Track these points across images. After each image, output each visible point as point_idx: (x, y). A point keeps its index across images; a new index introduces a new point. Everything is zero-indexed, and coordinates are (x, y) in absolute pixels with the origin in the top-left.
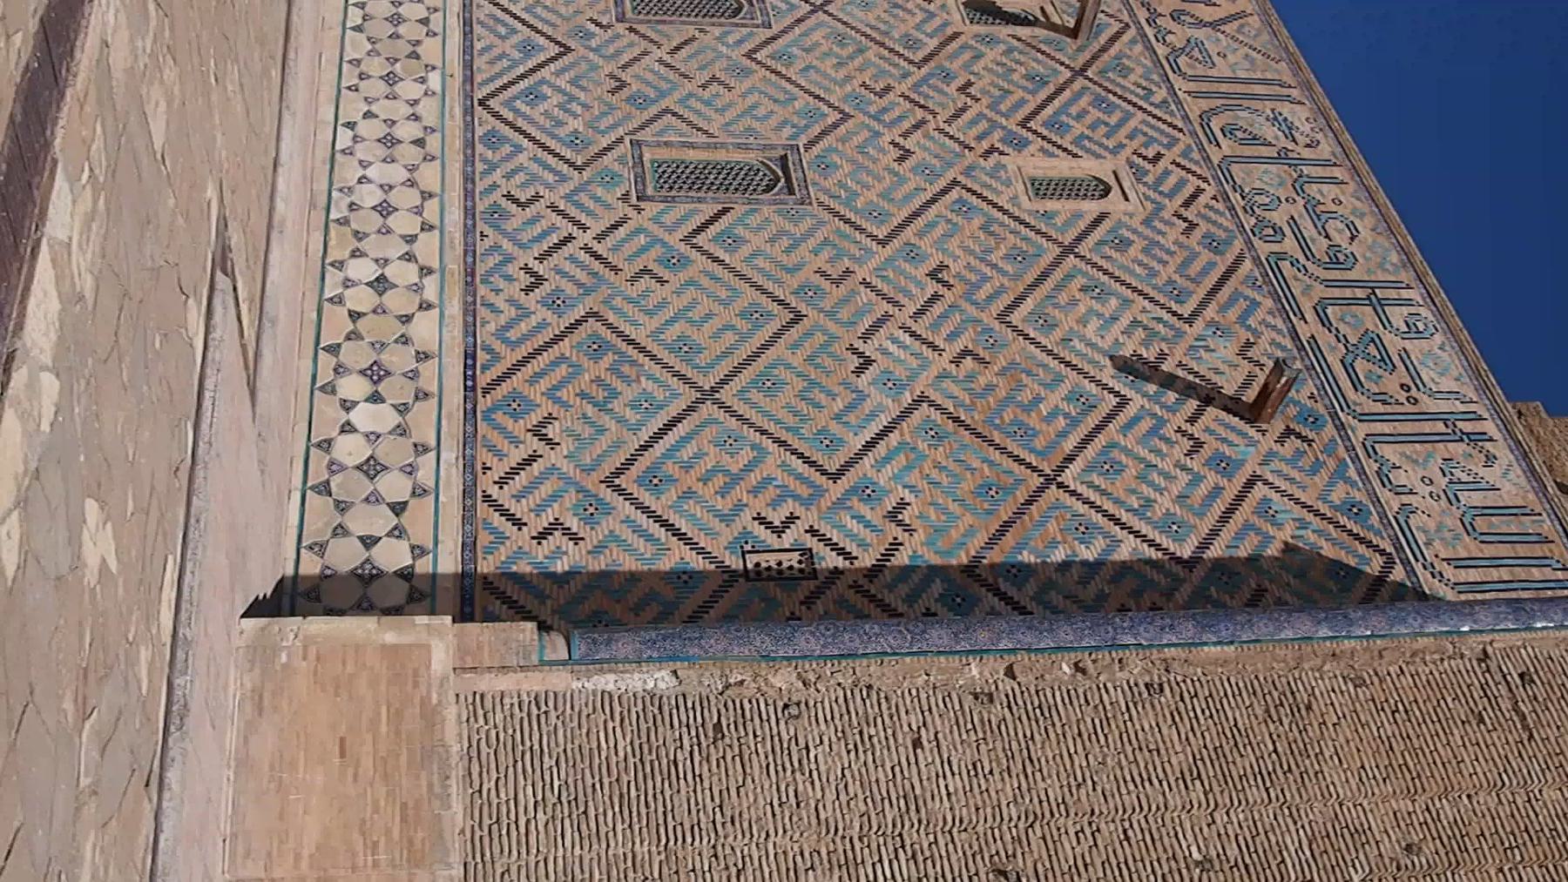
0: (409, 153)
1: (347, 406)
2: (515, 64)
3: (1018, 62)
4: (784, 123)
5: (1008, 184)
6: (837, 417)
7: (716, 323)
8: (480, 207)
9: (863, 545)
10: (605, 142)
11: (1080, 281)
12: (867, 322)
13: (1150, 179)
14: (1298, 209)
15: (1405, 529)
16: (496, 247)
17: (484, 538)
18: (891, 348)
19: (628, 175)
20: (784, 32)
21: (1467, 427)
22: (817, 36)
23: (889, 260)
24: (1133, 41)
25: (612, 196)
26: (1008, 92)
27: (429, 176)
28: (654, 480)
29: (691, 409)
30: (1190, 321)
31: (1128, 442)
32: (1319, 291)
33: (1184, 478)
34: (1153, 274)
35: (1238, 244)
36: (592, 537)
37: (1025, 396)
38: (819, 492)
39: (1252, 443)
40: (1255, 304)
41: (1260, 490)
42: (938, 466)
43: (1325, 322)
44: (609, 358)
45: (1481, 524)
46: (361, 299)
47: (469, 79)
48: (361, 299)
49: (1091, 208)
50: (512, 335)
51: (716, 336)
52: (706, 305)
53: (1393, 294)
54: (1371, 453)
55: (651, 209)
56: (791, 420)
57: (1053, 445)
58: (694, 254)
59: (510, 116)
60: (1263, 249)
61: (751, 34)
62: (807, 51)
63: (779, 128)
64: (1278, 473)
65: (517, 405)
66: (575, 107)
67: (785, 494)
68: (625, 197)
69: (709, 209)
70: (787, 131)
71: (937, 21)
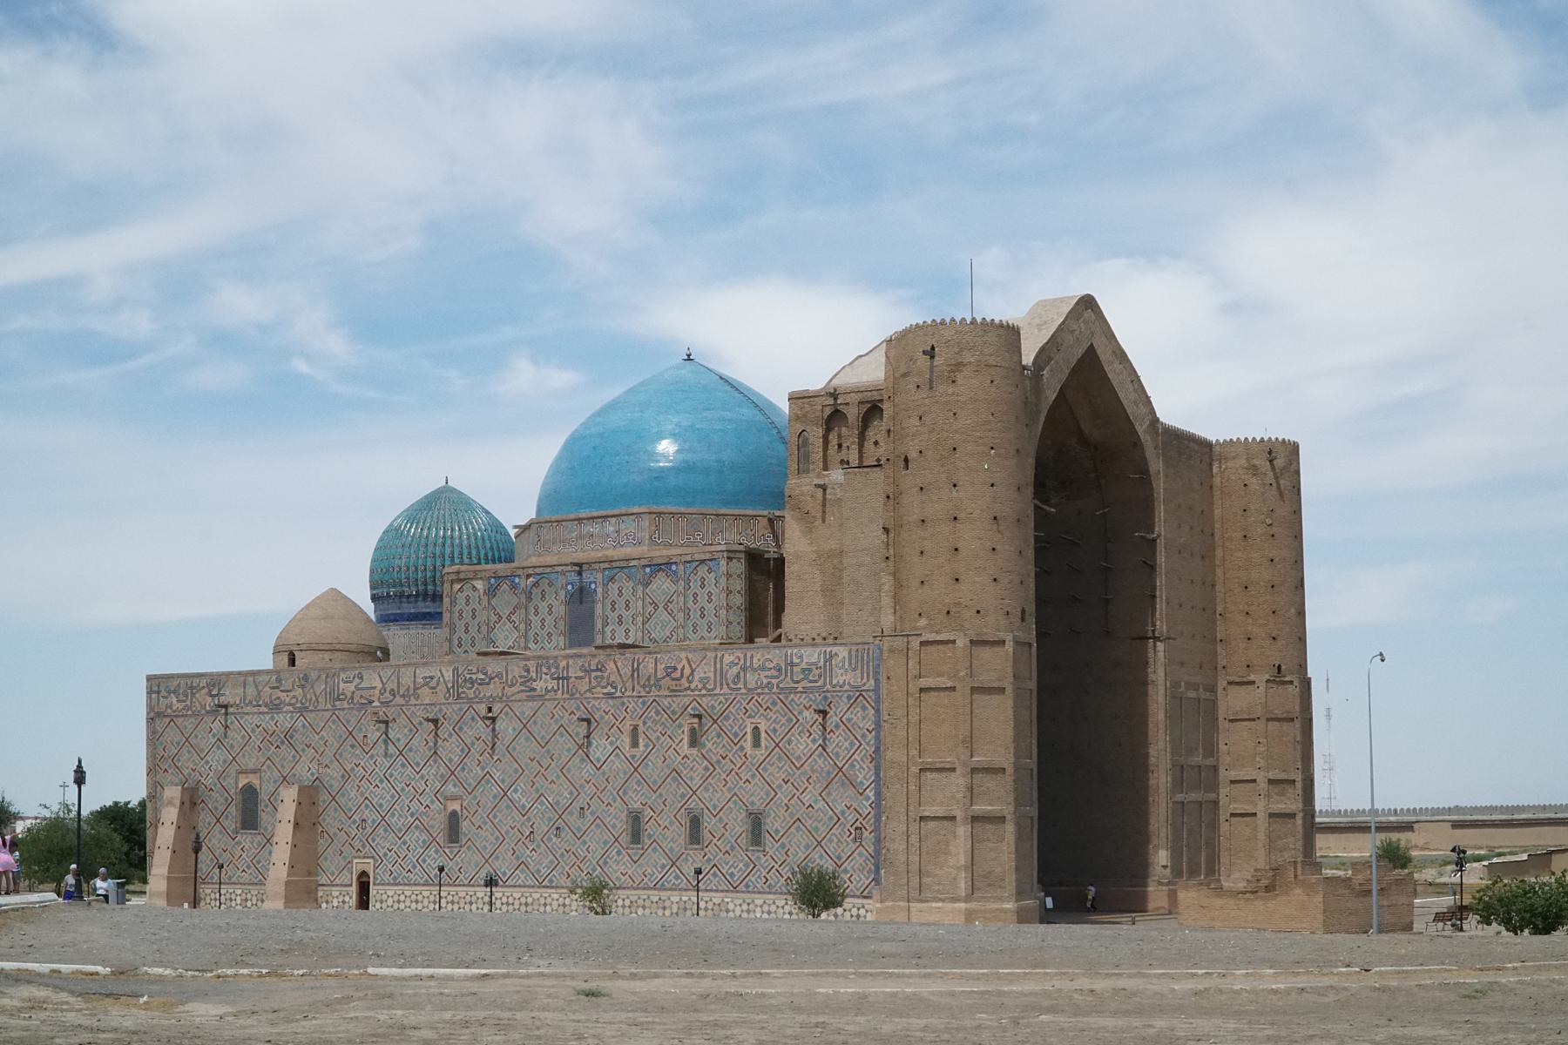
0: (752, 907)
3: (712, 739)
4: (738, 811)
5: (756, 755)
6: (825, 815)
8: (768, 890)
9: (855, 816)
10: (747, 859)
12: (799, 802)
13: (753, 714)
14: (763, 674)
15: (853, 687)
16: (780, 888)
18: (806, 798)
19: (757, 854)
20: (704, 804)
21: (828, 657)
22: (706, 796)
23: (782, 793)
24: (701, 699)
26: (724, 746)
27: (759, 902)
28: (839, 858)
29: (822, 847)
30: (798, 720)
31: (831, 748)
32: (788, 679)
33: (840, 738)
34: (783, 724)
36: (852, 872)
37: (819, 769)
38: (842, 823)
39: (831, 717)
40: (793, 700)
41: (844, 719)
42: (837, 795)
43: (798, 682)
47: (727, 891)
49: (763, 735)
51: (804, 839)
52: (795, 840)
53: (789, 658)
54: (834, 686)
55: (767, 849)
57: (832, 766)
59: (739, 882)
60: (775, 690)
61: (707, 814)
62: (711, 800)
63: (740, 813)
64: (840, 713)
66: (736, 864)
67: (843, 830)
68: (765, 856)
69: (767, 835)
70: (741, 811)
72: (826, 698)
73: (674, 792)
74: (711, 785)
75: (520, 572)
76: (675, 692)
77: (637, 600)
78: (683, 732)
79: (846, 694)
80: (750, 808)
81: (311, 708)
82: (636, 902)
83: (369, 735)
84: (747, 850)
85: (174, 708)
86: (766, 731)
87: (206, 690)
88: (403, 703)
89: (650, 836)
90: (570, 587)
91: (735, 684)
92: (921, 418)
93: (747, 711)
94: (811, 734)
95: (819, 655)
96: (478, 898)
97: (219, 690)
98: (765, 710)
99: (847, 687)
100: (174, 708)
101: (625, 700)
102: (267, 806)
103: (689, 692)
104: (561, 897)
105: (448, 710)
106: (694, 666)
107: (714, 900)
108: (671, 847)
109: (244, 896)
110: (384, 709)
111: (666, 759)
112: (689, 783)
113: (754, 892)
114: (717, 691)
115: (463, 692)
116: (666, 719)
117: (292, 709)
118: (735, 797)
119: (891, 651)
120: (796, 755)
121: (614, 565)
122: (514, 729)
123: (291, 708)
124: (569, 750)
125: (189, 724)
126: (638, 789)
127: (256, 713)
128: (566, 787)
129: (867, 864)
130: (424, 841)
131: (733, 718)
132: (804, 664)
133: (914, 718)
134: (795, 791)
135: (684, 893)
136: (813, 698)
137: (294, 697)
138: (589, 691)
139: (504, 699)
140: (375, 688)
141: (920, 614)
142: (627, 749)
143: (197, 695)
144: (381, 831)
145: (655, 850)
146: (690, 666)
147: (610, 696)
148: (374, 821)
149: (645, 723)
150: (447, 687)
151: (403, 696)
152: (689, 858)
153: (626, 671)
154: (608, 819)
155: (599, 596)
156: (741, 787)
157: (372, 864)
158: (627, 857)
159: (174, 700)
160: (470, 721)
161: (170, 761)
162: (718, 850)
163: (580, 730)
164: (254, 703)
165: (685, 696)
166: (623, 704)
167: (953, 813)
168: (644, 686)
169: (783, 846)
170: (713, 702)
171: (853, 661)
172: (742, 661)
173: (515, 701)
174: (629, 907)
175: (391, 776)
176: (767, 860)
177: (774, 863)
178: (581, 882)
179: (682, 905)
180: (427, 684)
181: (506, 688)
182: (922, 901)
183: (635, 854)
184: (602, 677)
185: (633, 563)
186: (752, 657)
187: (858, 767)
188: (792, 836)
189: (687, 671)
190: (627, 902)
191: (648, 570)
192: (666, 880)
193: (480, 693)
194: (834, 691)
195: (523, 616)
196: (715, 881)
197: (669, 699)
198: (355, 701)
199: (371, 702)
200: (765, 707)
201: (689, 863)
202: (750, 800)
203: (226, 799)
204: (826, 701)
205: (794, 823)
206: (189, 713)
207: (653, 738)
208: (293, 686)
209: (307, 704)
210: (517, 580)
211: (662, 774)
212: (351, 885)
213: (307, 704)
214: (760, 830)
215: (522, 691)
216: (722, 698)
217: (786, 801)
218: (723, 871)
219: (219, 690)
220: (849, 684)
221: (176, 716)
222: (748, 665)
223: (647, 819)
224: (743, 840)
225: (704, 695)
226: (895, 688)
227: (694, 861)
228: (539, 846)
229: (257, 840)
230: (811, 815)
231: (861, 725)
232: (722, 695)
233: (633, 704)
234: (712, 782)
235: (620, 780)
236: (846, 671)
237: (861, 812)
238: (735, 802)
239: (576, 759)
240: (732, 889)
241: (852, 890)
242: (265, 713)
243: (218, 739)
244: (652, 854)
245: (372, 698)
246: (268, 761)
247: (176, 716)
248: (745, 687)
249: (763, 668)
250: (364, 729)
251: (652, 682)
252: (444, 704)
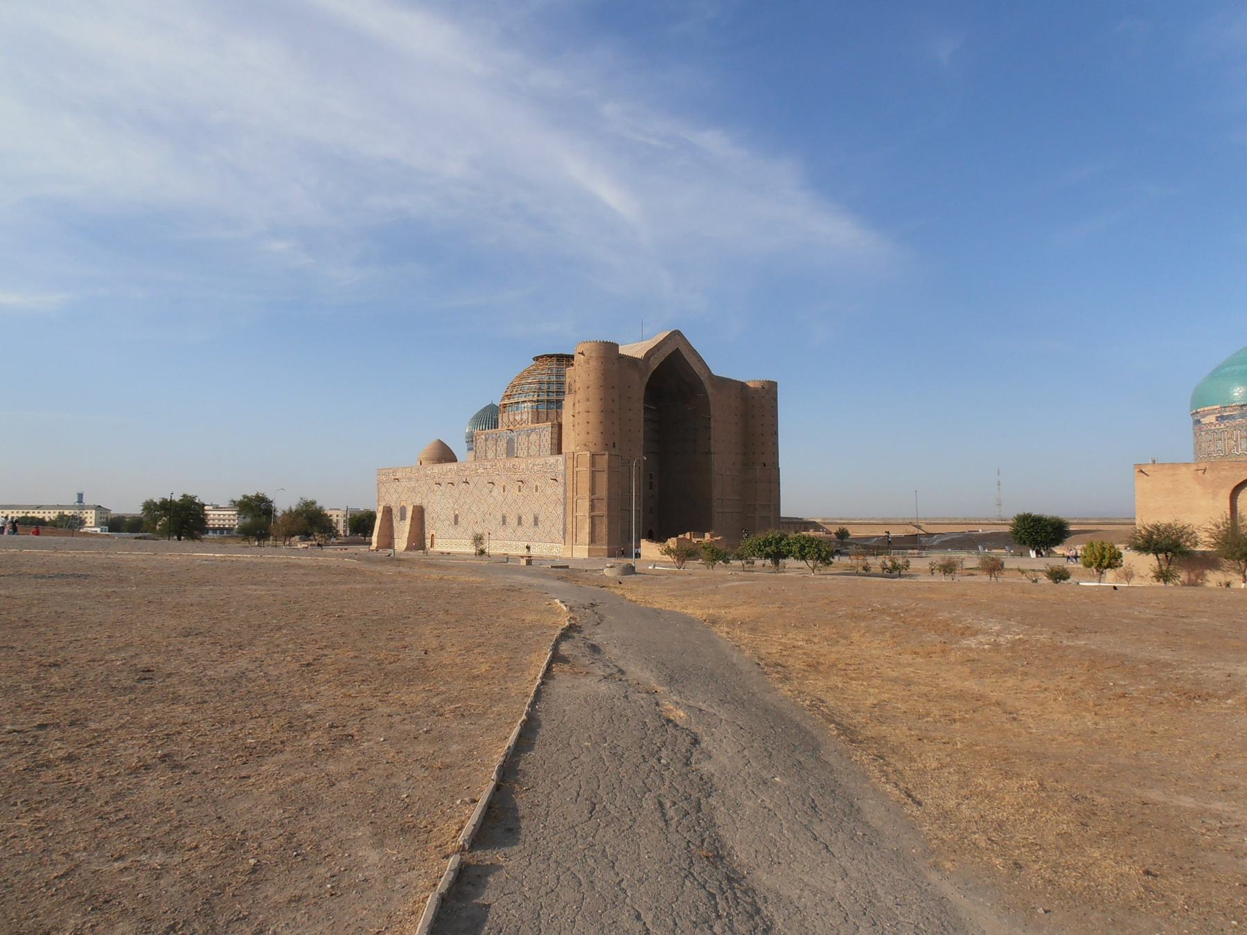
125: (387, 485)
133: (575, 482)
153: (502, 466)
155: (516, 440)
249: (538, 464)
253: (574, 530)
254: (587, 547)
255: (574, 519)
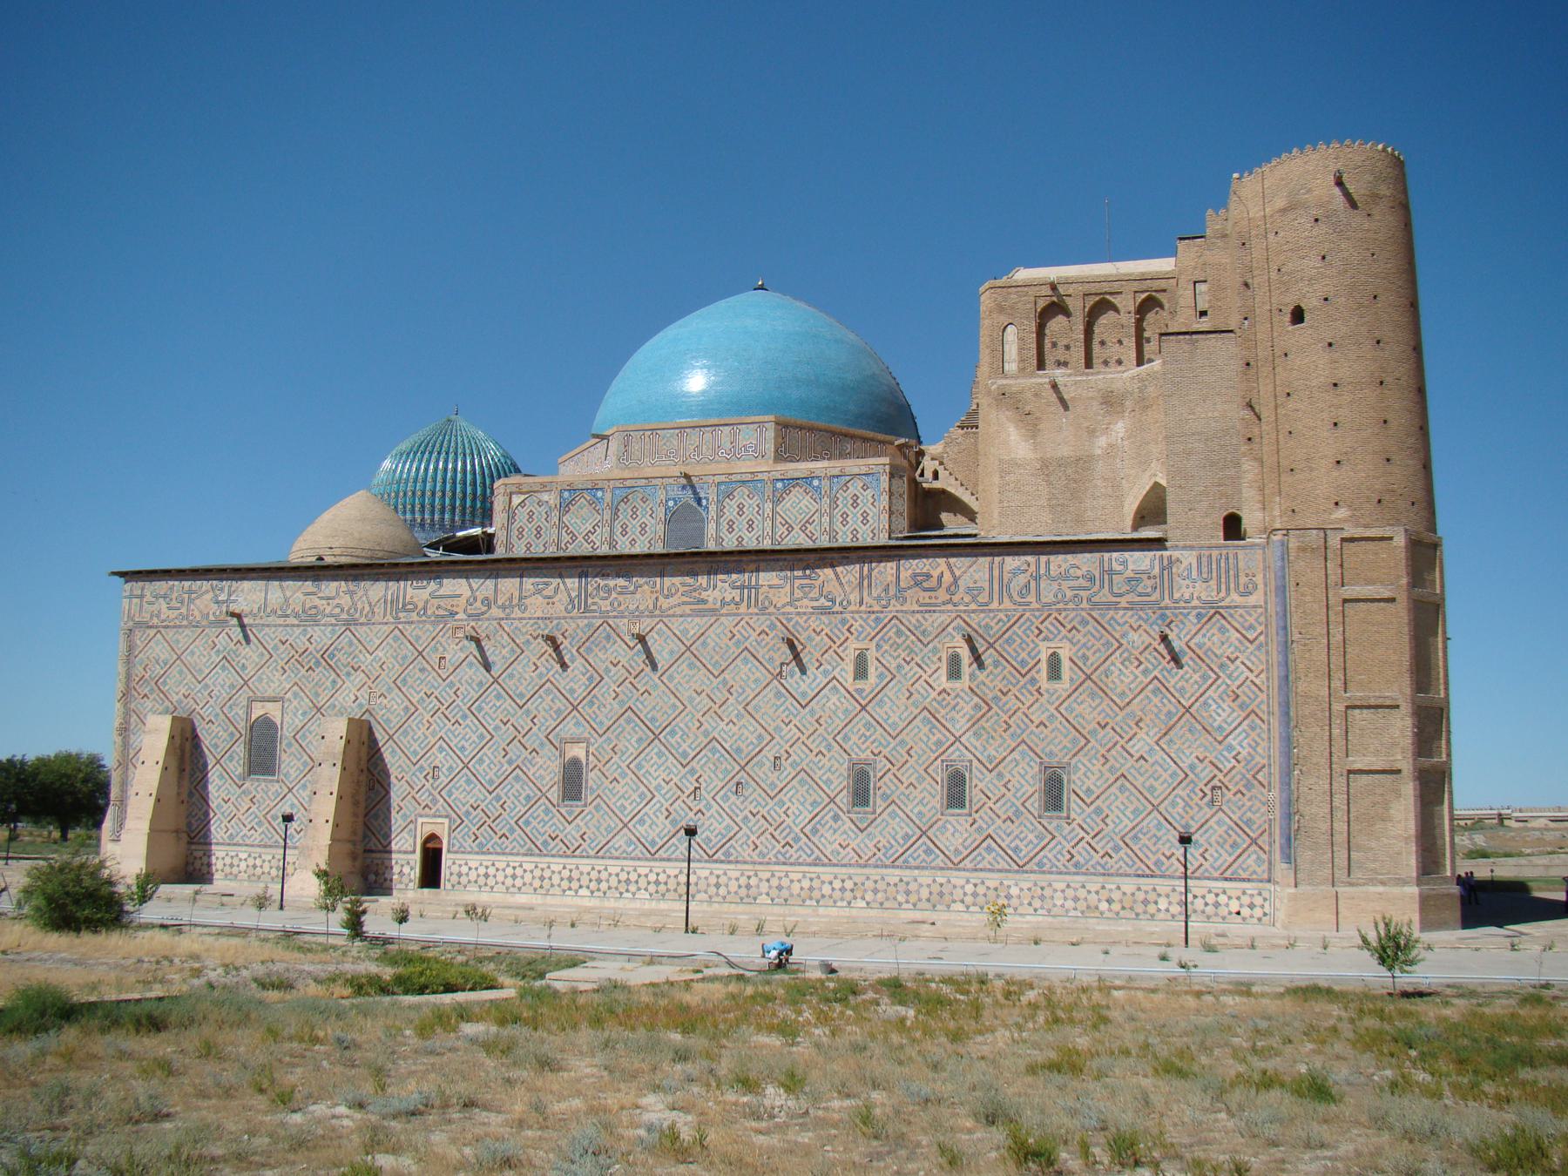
0: (1047, 892)
1: (1159, 910)
2: (998, 855)
5: (1056, 691)
7: (1126, 801)
11: (1103, 677)
12: (1125, 754)
13: (1051, 636)
14: (1066, 584)
17: (1207, 874)
18: (1137, 747)
19: (1055, 823)
21: (1166, 562)
22: (978, 744)
25: (1069, 828)
27: (1062, 886)
30: (1121, 645)
31: (1173, 682)
34: (1099, 650)
35: (1084, 614)
38: (1192, 781)
40: (1112, 618)
41: (1192, 644)
43: (1121, 595)
44: (1140, 835)
45: (1205, 576)
46: (1116, 907)
48: (1116, 907)
49: (1066, 665)
50: (1130, 863)
52: (1118, 803)
55: (1073, 815)
56: (1166, 785)
58: (1095, 805)
60: (1085, 605)
62: (985, 749)
65: (1158, 863)
69: (1073, 797)
71: (962, 694)
72: (1163, 617)
73: (925, 739)
74: (984, 728)
75: (605, 485)
76: (929, 609)
77: (764, 520)
78: (940, 659)
79: (1194, 612)
80: (1046, 759)
81: (363, 620)
82: (863, 884)
83: (448, 657)
84: (1040, 817)
85: (163, 617)
86: (1071, 659)
87: (211, 595)
88: (502, 615)
89: (885, 797)
90: (671, 503)
91: (1020, 594)
92: (1324, 258)
93: (1041, 632)
94: (1141, 663)
95: (1152, 561)
96: (610, 875)
97: (230, 595)
98: (1070, 631)
99: (1195, 602)
100: (163, 617)
101: (848, 616)
102: (289, 745)
103: (950, 607)
104: (742, 875)
105: (570, 626)
106: (958, 573)
107: (988, 883)
108: (920, 813)
109: (251, 862)
110: (473, 624)
111: (911, 694)
112: (949, 725)
113: (1050, 873)
114: (992, 606)
115: (594, 604)
116: (912, 642)
117: (334, 621)
118: (1023, 746)
119: (1302, 549)
120: (1119, 690)
121: (734, 478)
122: (672, 652)
123: (334, 621)
124: (756, 681)
125: (184, 638)
126: (868, 734)
127: (280, 625)
128: (751, 728)
129: (1230, 836)
130: (528, 798)
131: (1019, 641)
132: (1129, 571)
133: (1337, 638)
134: (1118, 738)
135: (939, 873)
136: (1144, 616)
137: (337, 606)
138: (788, 603)
139: (657, 612)
140: (460, 596)
141: (1337, 504)
142: (850, 679)
143: (197, 602)
144: (462, 782)
145: (893, 815)
146: (952, 572)
147: (825, 611)
148: (450, 769)
149: (878, 646)
150: (569, 596)
151: (503, 607)
152: (949, 826)
154: (820, 773)
156: (1032, 732)
157: (446, 825)
158: (849, 824)
159: (164, 606)
160: (604, 642)
161: (153, 684)
162: (994, 816)
163: (776, 656)
164: (279, 612)
165: (940, 611)
166: (844, 621)
167: (1398, 766)
168: (878, 599)
169: (1098, 811)
170: (987, 620)
171: (1205, 570)
172: (1033, 568)
173: (673, 616)
174: (852, 890)
175: (480, 709)
176: (1073, 829)
177: (1082, 834)
178: (775, 856)
179: (935, 888)
180: (539, 592)
181: (661, 598)
182: (1351, 884)
183: (861, 820)
184: (811, 587)
185: (760, 476)
186: (1048, 562)
187: (1214, 706)
188: (1113, 797)
189: (947, 578)
190: (849, 884)
191: (779, 485)
192: (911, 855)
193: (620, 605)
194: (1175, 608)
195: (606, 535)
196: (989, 858)
197: (918, 616)
198: (429, 612)
199: (452, 614)
200: (1069, 627)
201: (948, 834)
202: (1047, 750)
203: (232, 734)
204: (1164, 620)
205: (1117, 779)
206: (185, 623)
207: (892, 667)
208: (338, 594)
209: (357, 615)
210: (599, 494)
211: (906, 714)
212: (414, 852)
213: (357, 615)
214: (1061, 789)
215: (684, 603)
216: (1001, 615)
217: (1103, 751)
218: (1003, 845)
219: (230, 595)
220: (1199, 598)
221: (165, 627)
222: (1042, 571)
223: (880, 774)
224: (1035, 804)
225: (974, 611)
226: (1308, 598)
227: (956, 830)
228: (709, 807)
229: (273, 790)
230: (1142, 770)
231: (1218, 652)
232: (1000, 610)
233: (860, 622)
234: (986, 725)
235: (838, 721)
236: (1194, 581)
237: (1220, 766)
238: (1022, 753)
239: (769, 693)
240: (1016, 867)
241: (1207, 870)
242: (293, 625)
243: (224, 657)
244: (890, 821)
245: (455, 609)
246: (295, 688)
247: (165, 627)
248: (1038, 599)
250: (441, 649)
251: (892, 591)
252: (565, 618)
253: (1340, 826)
254: (1413, 890)
255: (1339, 784)
